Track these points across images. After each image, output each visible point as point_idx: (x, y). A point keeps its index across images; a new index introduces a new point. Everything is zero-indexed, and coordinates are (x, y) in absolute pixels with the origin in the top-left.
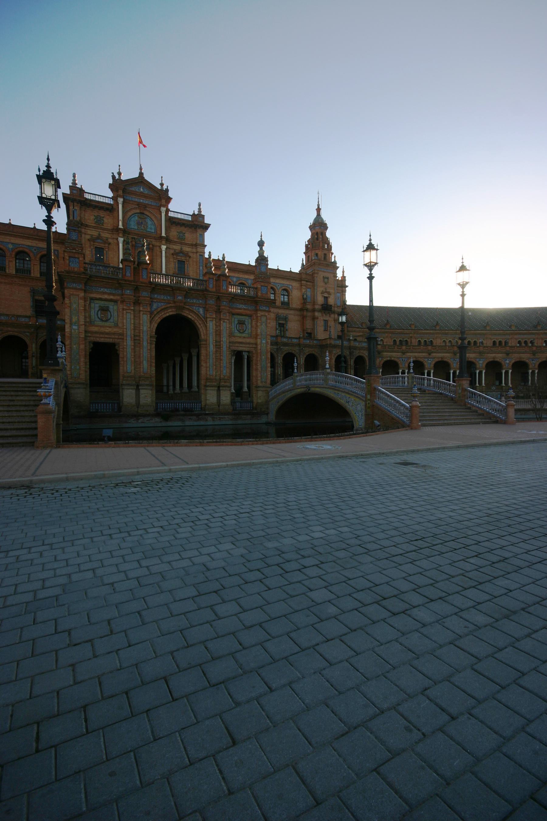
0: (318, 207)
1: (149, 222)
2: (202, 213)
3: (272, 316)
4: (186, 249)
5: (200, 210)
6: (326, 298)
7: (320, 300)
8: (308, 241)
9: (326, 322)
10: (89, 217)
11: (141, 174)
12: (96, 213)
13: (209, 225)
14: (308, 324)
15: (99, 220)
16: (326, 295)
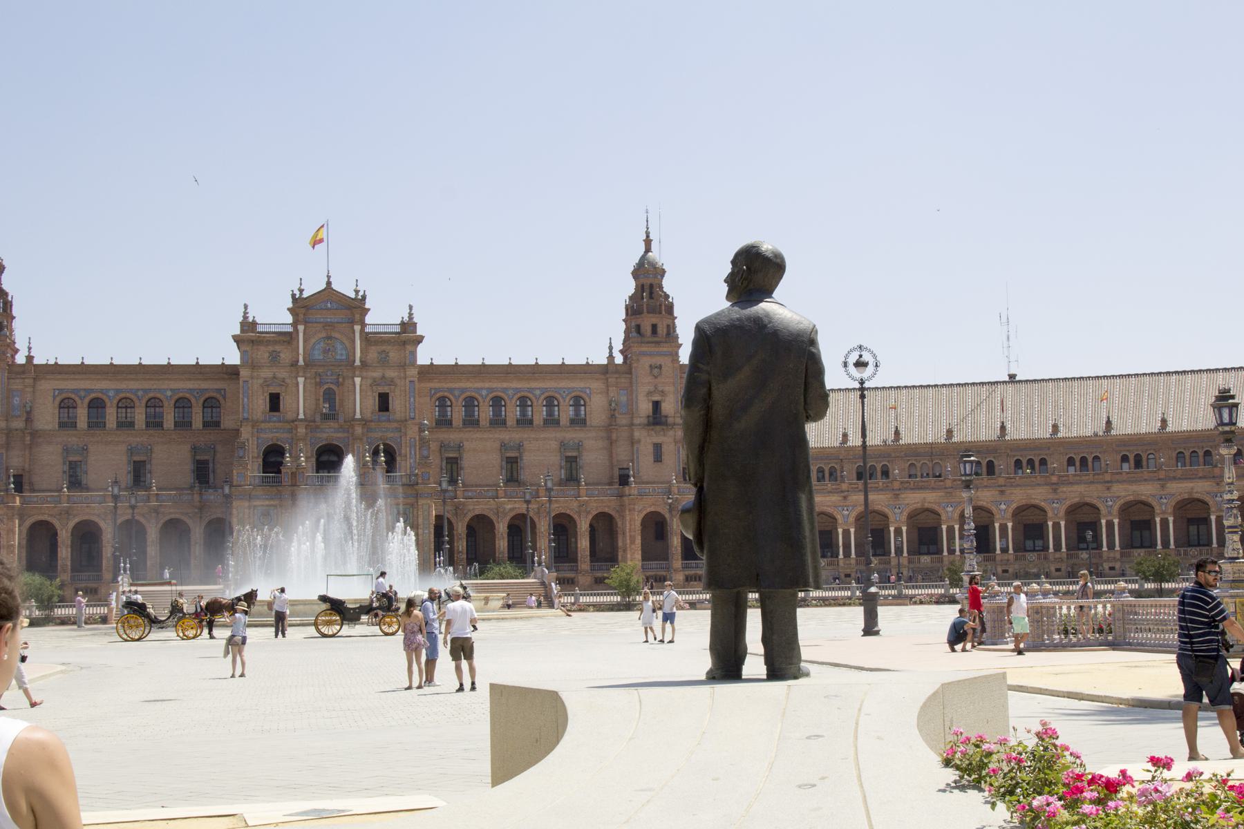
0: (648, 236)
1: (339, 346)
2: (415, 320)
3: (554, 445)
4: (391, 374)
5: (411, 314)
6: (656, 405)
7: (645, 407)
8: (631, 298)
9: (658, 449)
10: (262, 354)
11: (329, 283)
12: (271, 348)
13: (422, 337)
14: (622, 453)
15: (274, 357)
16: (656, 398)
